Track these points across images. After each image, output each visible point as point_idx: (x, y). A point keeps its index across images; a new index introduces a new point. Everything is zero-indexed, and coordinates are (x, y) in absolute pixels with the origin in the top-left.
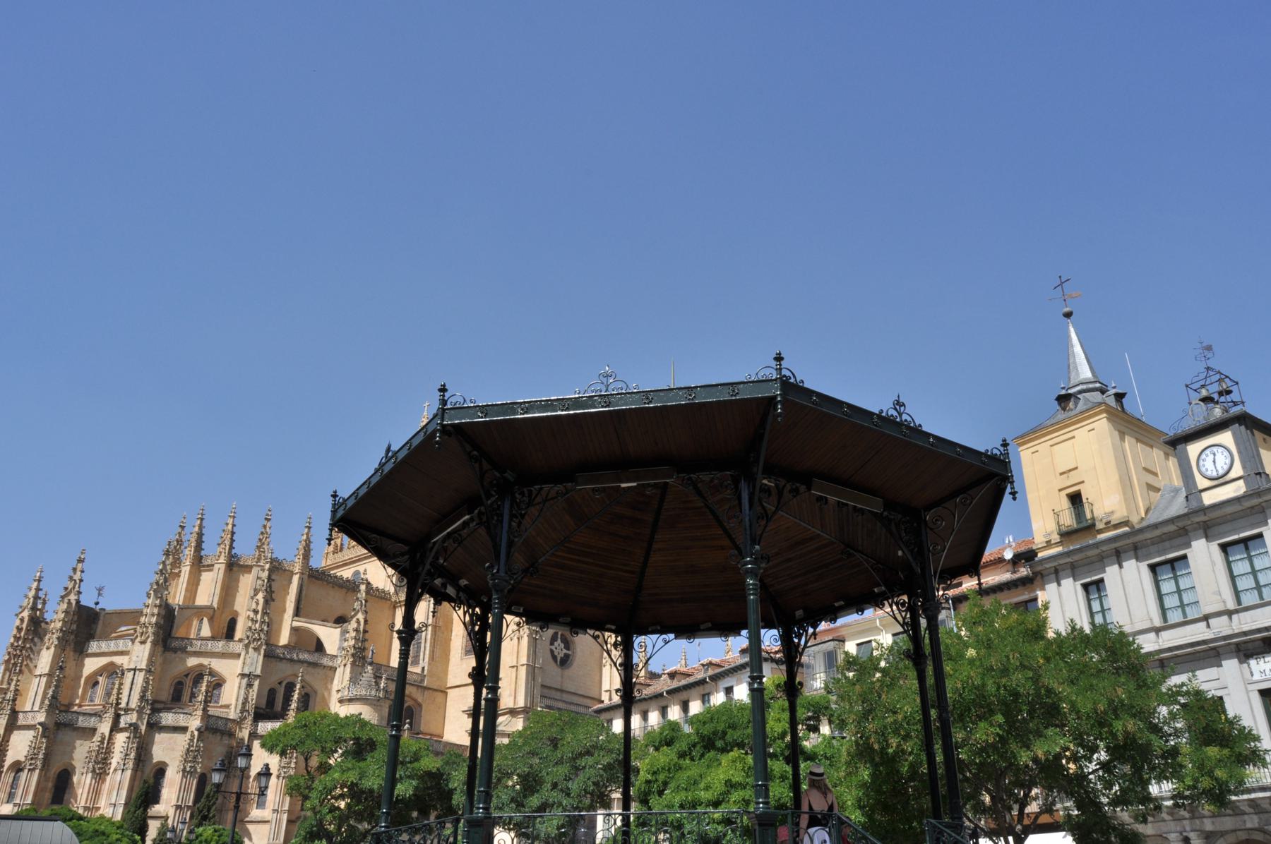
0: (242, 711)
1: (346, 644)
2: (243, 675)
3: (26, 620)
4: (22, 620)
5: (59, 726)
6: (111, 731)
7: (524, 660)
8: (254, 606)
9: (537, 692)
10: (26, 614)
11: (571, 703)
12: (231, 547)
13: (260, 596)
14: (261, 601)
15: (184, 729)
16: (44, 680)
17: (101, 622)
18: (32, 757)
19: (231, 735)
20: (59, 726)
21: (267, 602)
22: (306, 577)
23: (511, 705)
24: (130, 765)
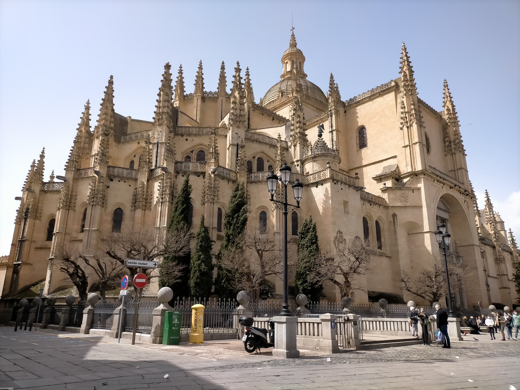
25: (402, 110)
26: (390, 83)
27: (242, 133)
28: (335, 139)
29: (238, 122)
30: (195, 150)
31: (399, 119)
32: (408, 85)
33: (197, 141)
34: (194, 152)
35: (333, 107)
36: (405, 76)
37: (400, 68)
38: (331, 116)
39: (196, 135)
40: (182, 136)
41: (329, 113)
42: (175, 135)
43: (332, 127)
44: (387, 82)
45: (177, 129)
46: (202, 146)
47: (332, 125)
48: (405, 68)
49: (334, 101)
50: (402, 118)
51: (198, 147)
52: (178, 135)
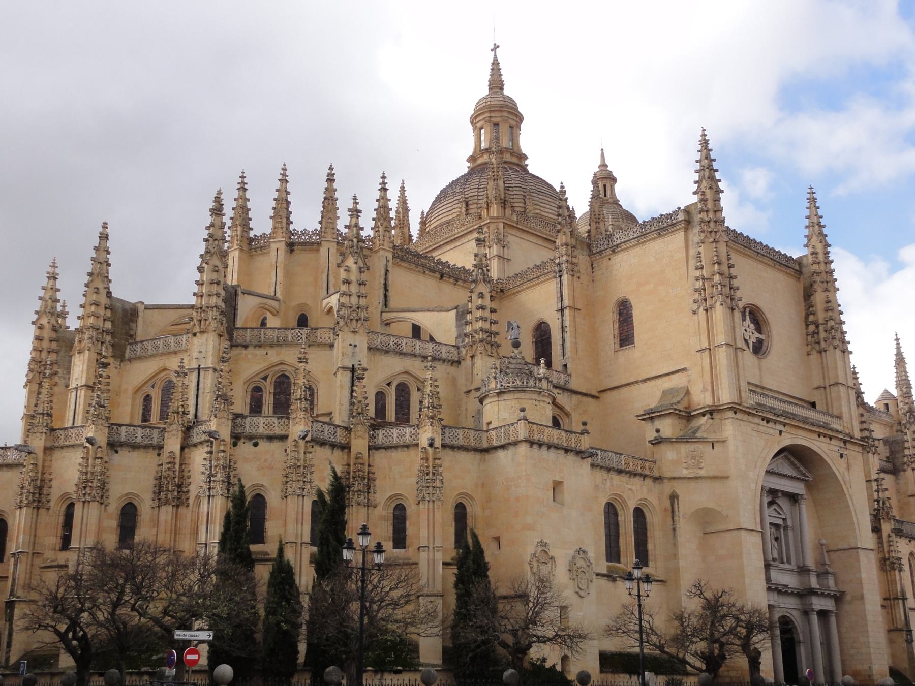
0: (351, 415)
1: (468, 329)
2: (344, 368)
3: (47, 326)
4: (41, 328)
5: (113, 446)
6: (182, 449)
7: (721, 338)
8: (343, 275)
9: (744, 387)
10: (44, 321)
11: (785, 402)
12: (289, 222)
13: (350, 262)
14: (354, 267)
15: (284, 438)
16: (82, 393)
17: (140, 320)
18: (84, 484)
19: (345, 447)
20: (113, 446)
21: (361, 271)
22: (390, 256)
23: (710, 403)
24: (219, 488)
25: (698, 273)
26: (676, 213)
27: (362, 341)
28: (567, 323)
29: (354, 321)
30: (271, 374)
31: (691, 291)
32: (709, 222)
33: (274, 356)
34: (269, 380)
35: (564, 258)
36: (703, 200)
37: (696, 182)
38: (560, 277)
39: (272, 346)
40: (246, 347)
41: (557, 269)
42: (232, 346)
43: (562, 300)
44: (670, 211)
45: (235, 333)
46: (284, 366)
47: (562, 295)
48: (704, 183)
49: (567, 245)
50: (696, 290)
51: (277, 368)
52: (237, 346)
